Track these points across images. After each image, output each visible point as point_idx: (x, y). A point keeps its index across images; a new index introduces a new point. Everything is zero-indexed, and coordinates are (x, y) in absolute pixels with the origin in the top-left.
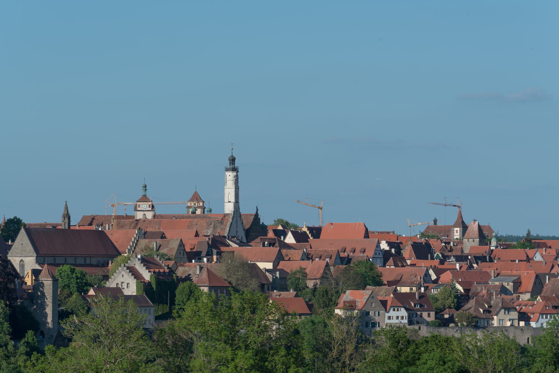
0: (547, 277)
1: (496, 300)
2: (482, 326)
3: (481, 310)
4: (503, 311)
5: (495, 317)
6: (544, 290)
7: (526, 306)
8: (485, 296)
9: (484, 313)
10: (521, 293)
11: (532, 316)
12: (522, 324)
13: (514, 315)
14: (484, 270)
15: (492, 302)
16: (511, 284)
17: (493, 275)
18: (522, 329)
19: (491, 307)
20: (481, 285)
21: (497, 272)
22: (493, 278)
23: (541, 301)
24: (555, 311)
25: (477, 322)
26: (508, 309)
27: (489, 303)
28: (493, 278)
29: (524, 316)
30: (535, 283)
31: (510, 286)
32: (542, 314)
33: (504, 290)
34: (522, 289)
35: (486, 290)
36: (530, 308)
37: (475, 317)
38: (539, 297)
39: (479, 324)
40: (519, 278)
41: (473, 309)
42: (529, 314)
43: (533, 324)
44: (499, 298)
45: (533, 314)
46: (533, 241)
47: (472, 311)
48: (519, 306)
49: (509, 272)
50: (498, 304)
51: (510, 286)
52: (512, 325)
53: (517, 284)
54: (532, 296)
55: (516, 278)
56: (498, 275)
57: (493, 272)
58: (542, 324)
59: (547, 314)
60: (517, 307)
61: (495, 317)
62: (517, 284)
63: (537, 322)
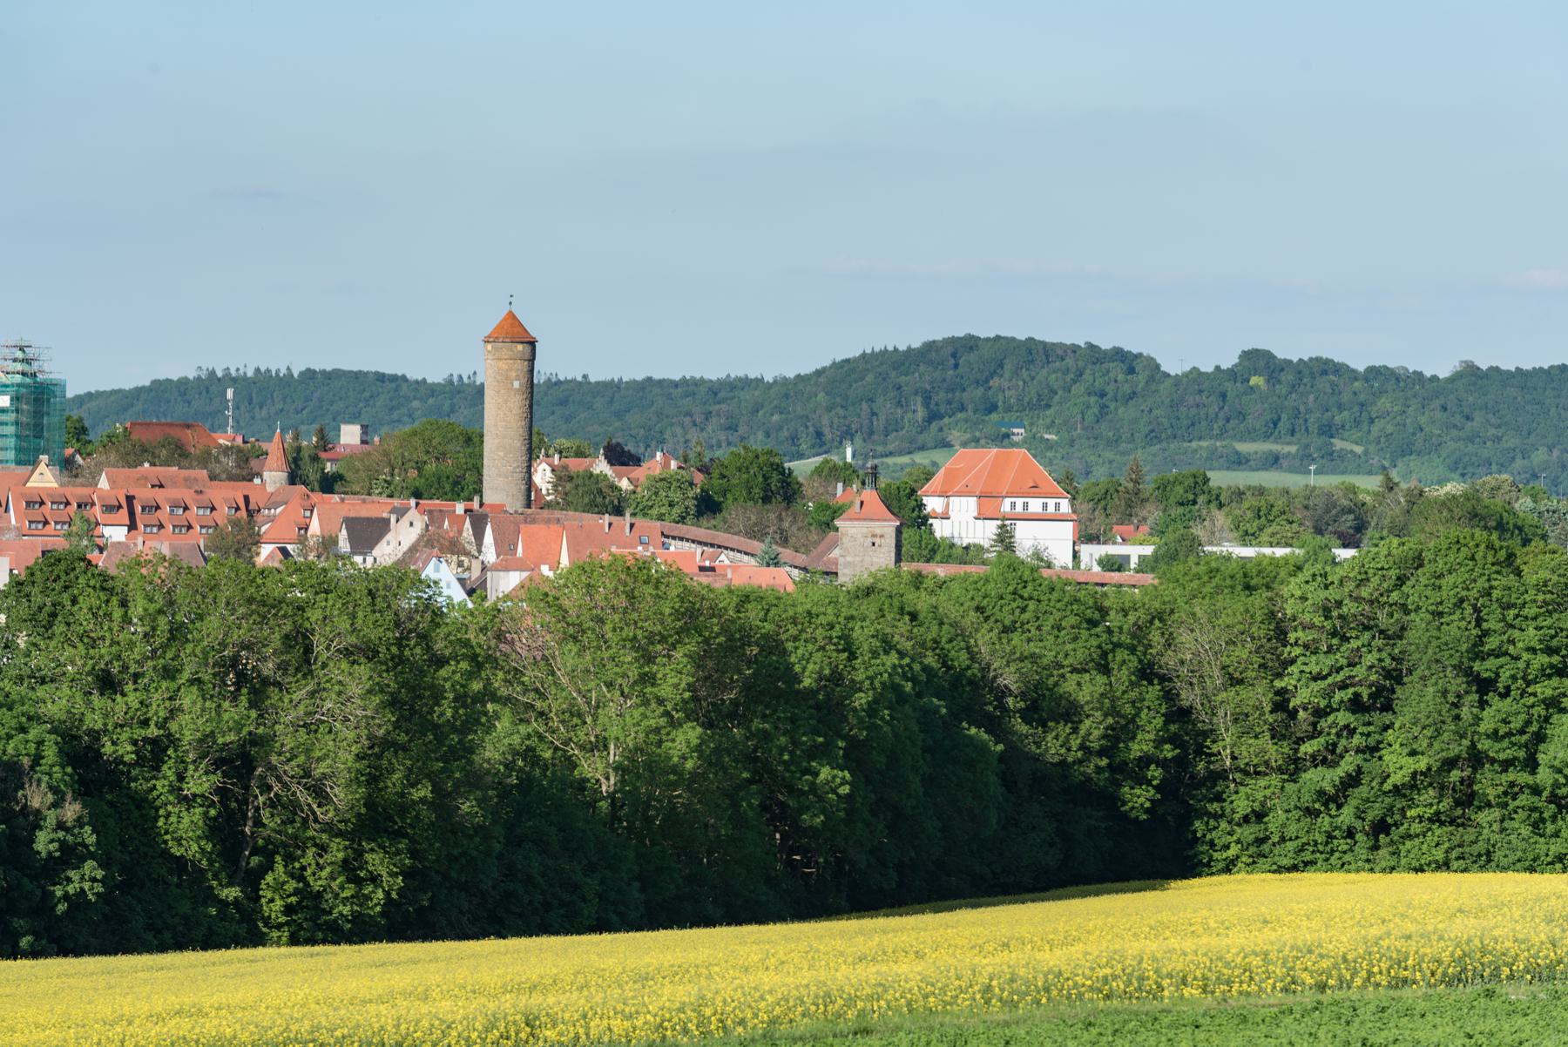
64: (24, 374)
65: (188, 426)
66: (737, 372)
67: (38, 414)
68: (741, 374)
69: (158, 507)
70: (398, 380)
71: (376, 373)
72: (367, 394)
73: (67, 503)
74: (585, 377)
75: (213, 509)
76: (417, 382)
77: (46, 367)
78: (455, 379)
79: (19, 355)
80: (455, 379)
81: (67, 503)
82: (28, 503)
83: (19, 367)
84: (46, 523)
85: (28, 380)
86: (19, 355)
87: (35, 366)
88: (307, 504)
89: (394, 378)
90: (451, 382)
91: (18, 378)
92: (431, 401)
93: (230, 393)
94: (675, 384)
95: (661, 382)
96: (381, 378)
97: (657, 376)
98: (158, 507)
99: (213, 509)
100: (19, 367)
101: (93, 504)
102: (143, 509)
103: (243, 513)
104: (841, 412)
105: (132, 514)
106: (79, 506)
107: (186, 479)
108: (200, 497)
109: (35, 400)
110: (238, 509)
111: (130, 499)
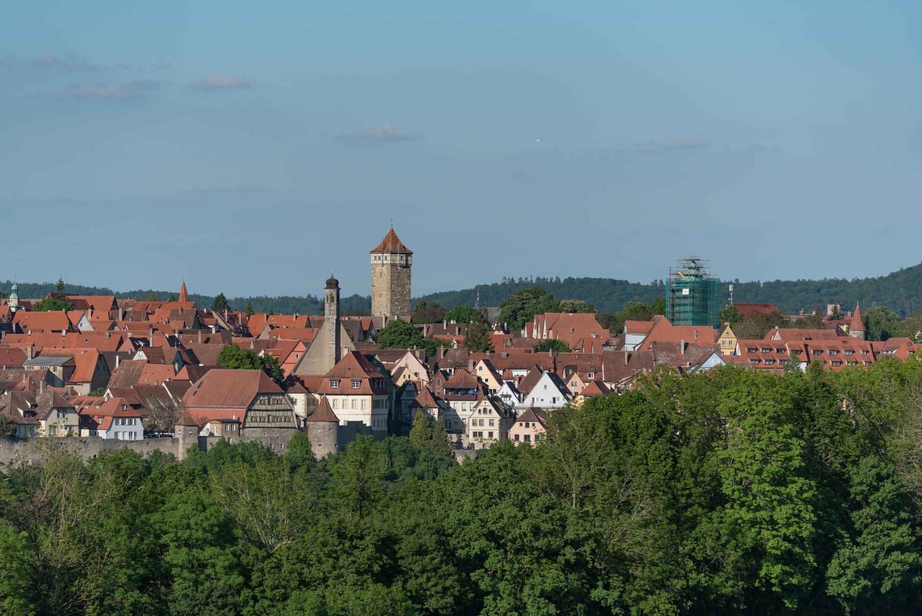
0: (117, 357)
1: (44, 394)
2: (21, 436)
3: (21, 412)
4: (55, 412)
5: (43, 423)
6: (113, 378)
7: (90, 404)
8: (27, 389)
9: (25, 416)
10: (75, 383)
11: (100, 421)
12: (85, 433)
13: (73, 419)
14: (12, 346)
15: (38, 399)
16: (60, 369)
17: (29, 354)
18: (84, 441)
19: (36, 406)
20: (13, 371)
21: (36, 349)
22: (29, 359)
23: (111, 396)
24: (135, 413)
25: (15, 430)
26: (63, 409)
27: (32, 400)
28: (29, 359)
29: (87, 422)
30: (97, 368)
31: (59, 372)
32: (117, 418)
33: (50, 379)
34: (76, 377)
35: (28, 379)
36: (98, 407)
37: (12, 422)
38: (108, 391)
39: (17, 434)
40: (72, 359)
41: (7, 408)
42: (95, 418)
43: (102, 434)
44: (50, 392)
45: (103, 417)
46: (71, 297)
47: (6, 412)
48: (80, 404)
49: (56, 351)
50: (47, 401)
51: (59, 372)
52: (70, 435)
53: (70, 368)
54: (93, 388)
55: (68, 359)
56: (38, 354)
57: (29, 349)
58: (116, 434)
59: (124, 418)
60: (77, 407)
61: (43, 423)
62: (70, 368)
63: (109, 430)
64: (696, 276)
65: (766, 306)
66: (830, 276)
67: (705, 299)
68: (832, 278)
69: (822, 351)
70: (625, 283)
71: (611, 280)
72: (606, 292)
73: (771, 350)
74: (737, 280)
75: (854, 352)
76: (634, 285)
77: (707, 271)
78: (658, 282)
79: (693, 265)
80: (658, 282)
81: (771, 350)
82: (749, 350)
83: (693, 272)
84: (760, 361)
85: (698, 280)
86: (693, 265)
87: (701, 272)
88: (910, 348)
89: (621, 282)
90: (655, 284)
91: (693, 278)
92: (645, 296)
93: (731, 288)
94: (795, 284)
95: (786, 283)
96: (613, 282)
97: (783, 279)
98: (822, 351)
99: (854, 352)
100: (693, 272)
101: (786, 350)
102: (814, 351)
103: (870, 354)
104: (916, 299)
105: (808, 355)
106: (778, 351)
107: (824, 335)
108: (845, 345)
109: (703, 291)
110: (868, 352)
111: (806, 346)
